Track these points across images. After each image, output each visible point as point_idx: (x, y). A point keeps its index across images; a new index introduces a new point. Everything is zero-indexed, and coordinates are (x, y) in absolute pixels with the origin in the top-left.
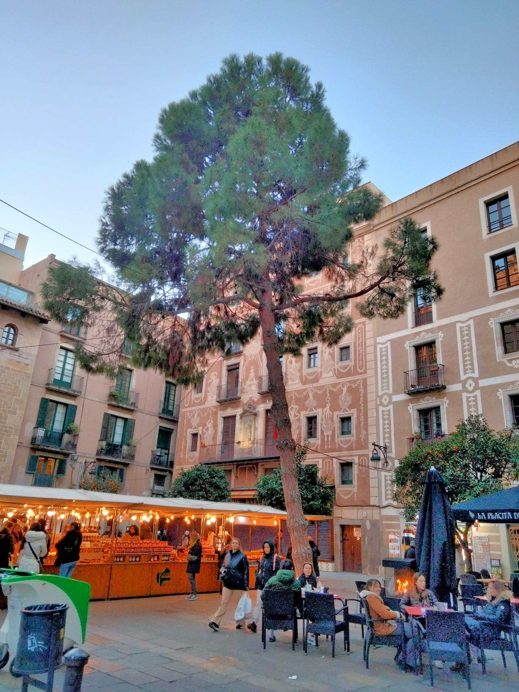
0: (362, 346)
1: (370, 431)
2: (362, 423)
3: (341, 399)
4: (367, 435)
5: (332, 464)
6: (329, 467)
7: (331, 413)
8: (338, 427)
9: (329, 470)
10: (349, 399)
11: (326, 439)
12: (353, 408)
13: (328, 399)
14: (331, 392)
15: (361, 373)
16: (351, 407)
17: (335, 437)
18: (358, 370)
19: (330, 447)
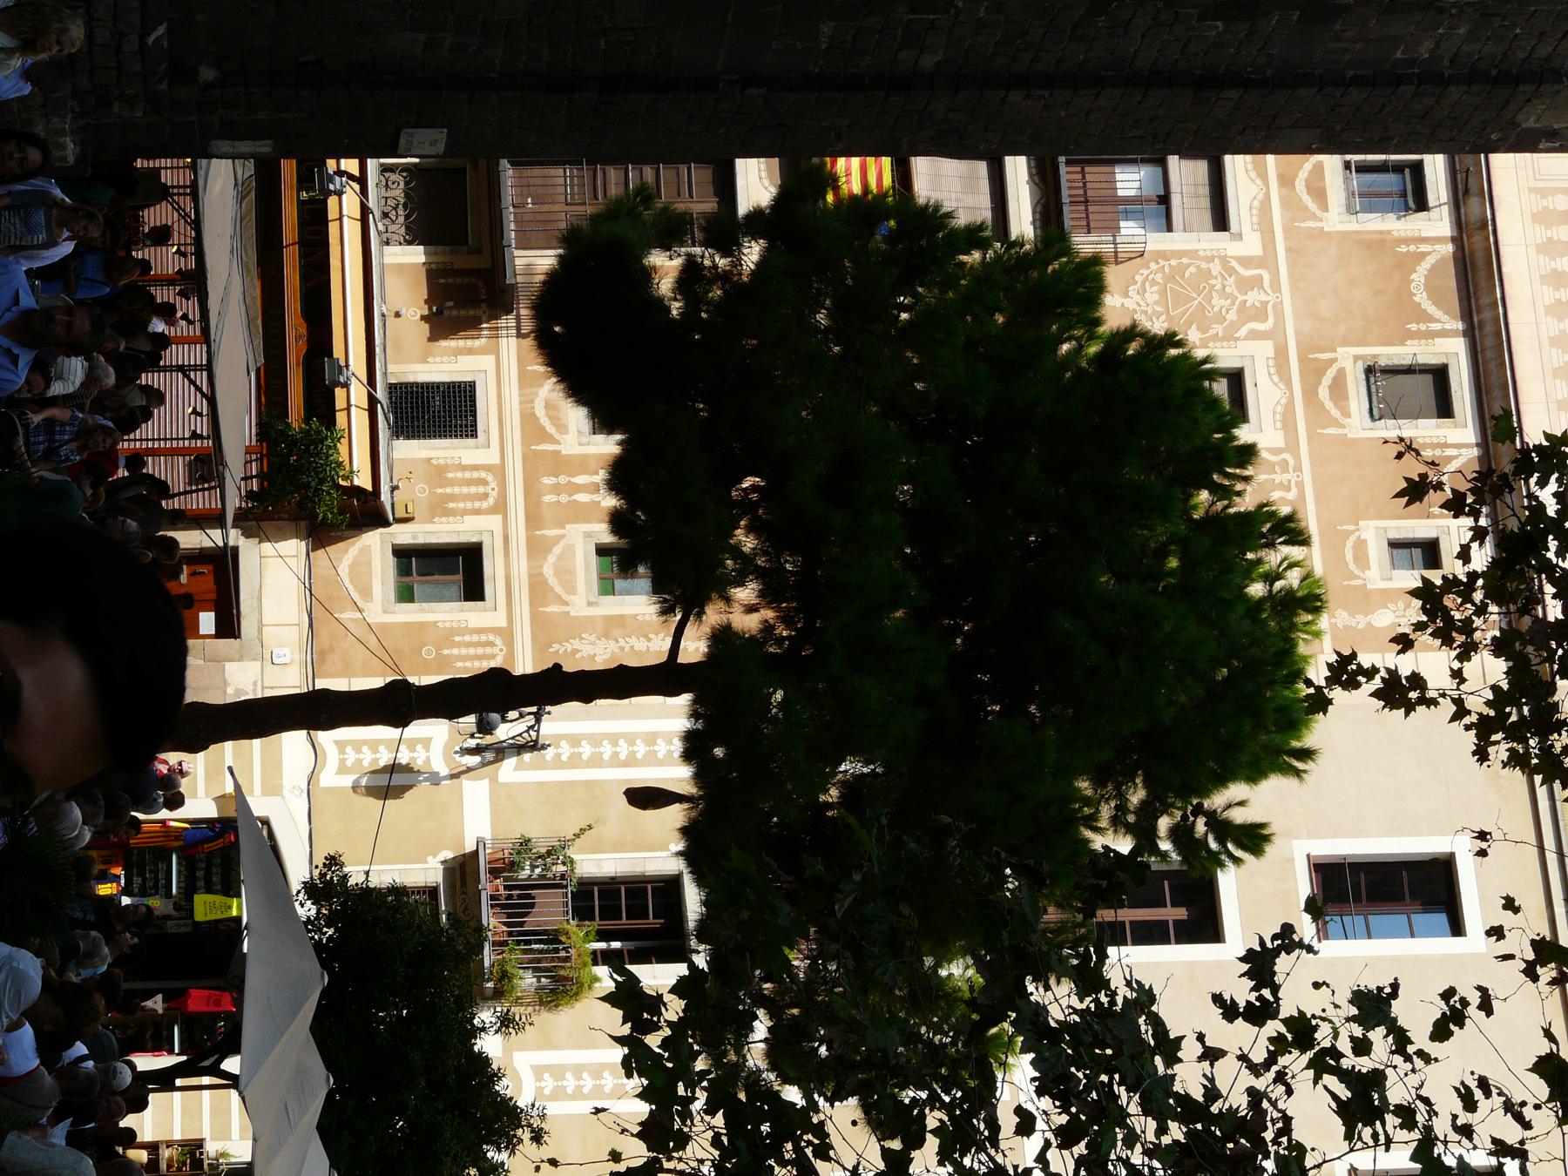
5: (477, 512)
6: (465, 497)
17: (587, 521)
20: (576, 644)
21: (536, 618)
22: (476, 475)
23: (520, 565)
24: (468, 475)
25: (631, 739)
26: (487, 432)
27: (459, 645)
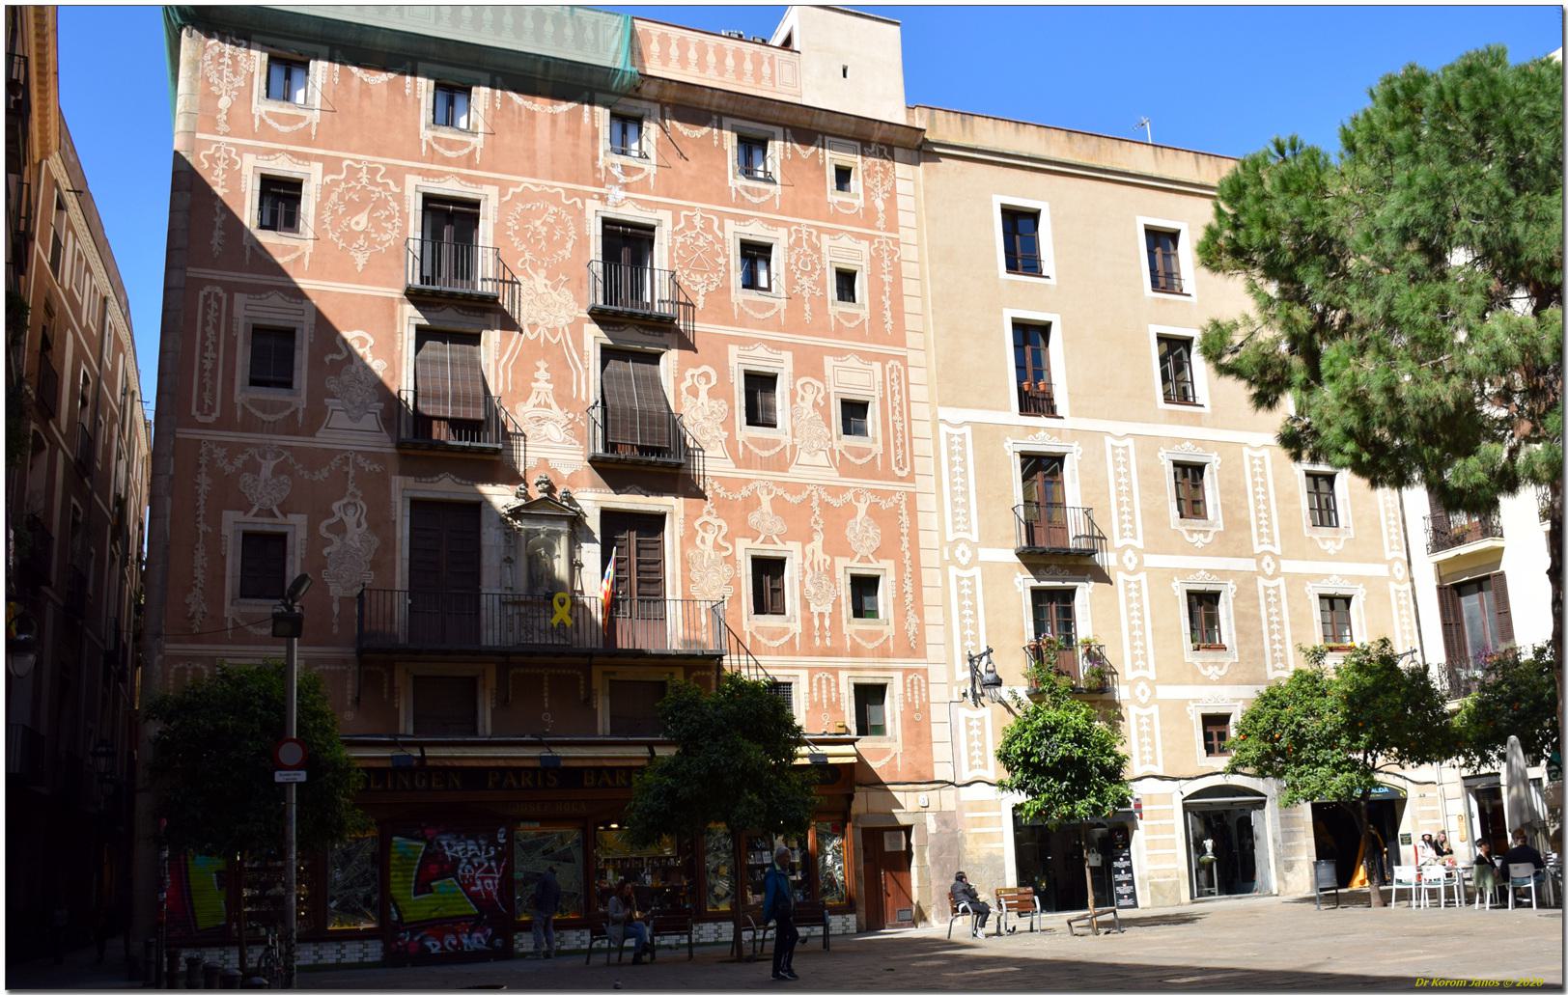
1: (928, 618)
2: (909, 598)
4: (921, 627)
6: (829, 692)
9: (829, 699)
11: (816, 623)
14: (825, 506)
15: (901, 479)
16: (879, 553)
19: (828, 642)
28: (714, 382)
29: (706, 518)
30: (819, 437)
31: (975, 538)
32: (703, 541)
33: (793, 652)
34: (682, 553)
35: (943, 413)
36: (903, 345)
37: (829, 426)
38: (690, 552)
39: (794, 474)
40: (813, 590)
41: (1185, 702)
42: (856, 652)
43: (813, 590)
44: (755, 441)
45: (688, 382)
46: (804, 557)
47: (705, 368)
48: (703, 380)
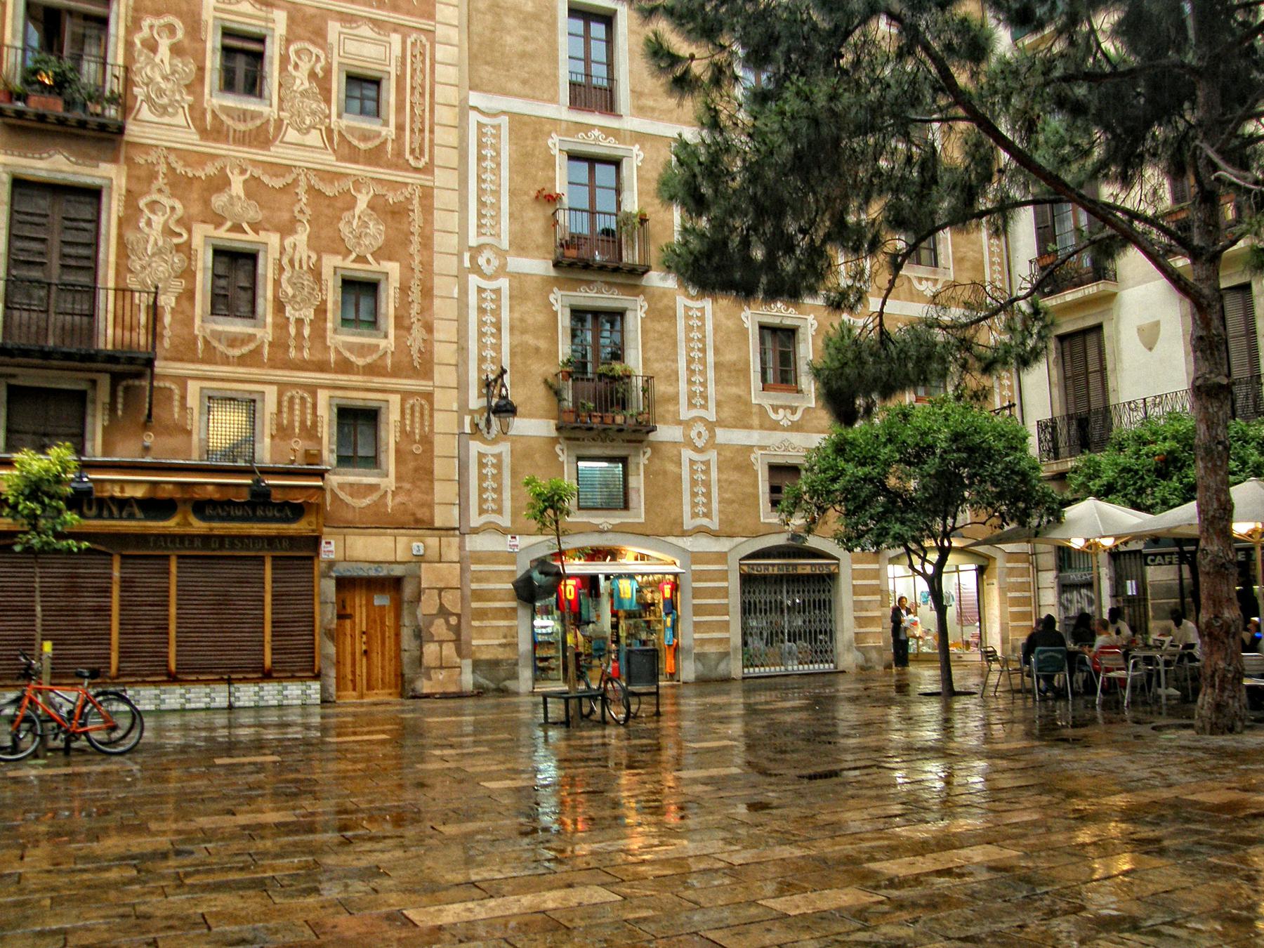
0: (422, 95)
1: (437, 336)
2: (415, 308)
3: (350, 223)
4: (428, 343)
5: (315, 406)
6: (303, 413)
7: (314, 257)
8: (335, 303)
9: (303, 422)
10: (376, 232)
12: (390, 259)
13: (301, 211)
14: (311, 189)
15: (416, 170)
16: (382, 253)
17: (325, 330)
18: (408, 156)
20: (414, 352)
21: (396, 372)
22: (285, 404)
23: (357, 380)
24: (285, 409)
25: (481, 324)
26: (250, 392)
27: (412, 427)
28: (180, 34)
29: (156, 197)
30: (313, 113)
31: (505, 244)
32: (149, 223)
33: (260, 365)
34: (120, 236)
35: (475, 99)
36: (431, 16)
37: (328, 101)
38: (130, 236)
39: (276, 154)
40: (290, 291)
41: (750, 448)
42: (345, 366)
43: (290, 291)
44: (228, 111)
45: (146, 32)
46: (283, 250)
47: (170, 19)
48: (165, 34)
